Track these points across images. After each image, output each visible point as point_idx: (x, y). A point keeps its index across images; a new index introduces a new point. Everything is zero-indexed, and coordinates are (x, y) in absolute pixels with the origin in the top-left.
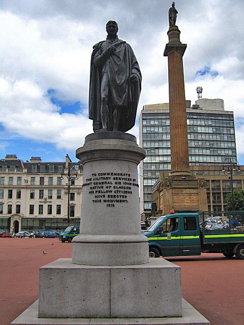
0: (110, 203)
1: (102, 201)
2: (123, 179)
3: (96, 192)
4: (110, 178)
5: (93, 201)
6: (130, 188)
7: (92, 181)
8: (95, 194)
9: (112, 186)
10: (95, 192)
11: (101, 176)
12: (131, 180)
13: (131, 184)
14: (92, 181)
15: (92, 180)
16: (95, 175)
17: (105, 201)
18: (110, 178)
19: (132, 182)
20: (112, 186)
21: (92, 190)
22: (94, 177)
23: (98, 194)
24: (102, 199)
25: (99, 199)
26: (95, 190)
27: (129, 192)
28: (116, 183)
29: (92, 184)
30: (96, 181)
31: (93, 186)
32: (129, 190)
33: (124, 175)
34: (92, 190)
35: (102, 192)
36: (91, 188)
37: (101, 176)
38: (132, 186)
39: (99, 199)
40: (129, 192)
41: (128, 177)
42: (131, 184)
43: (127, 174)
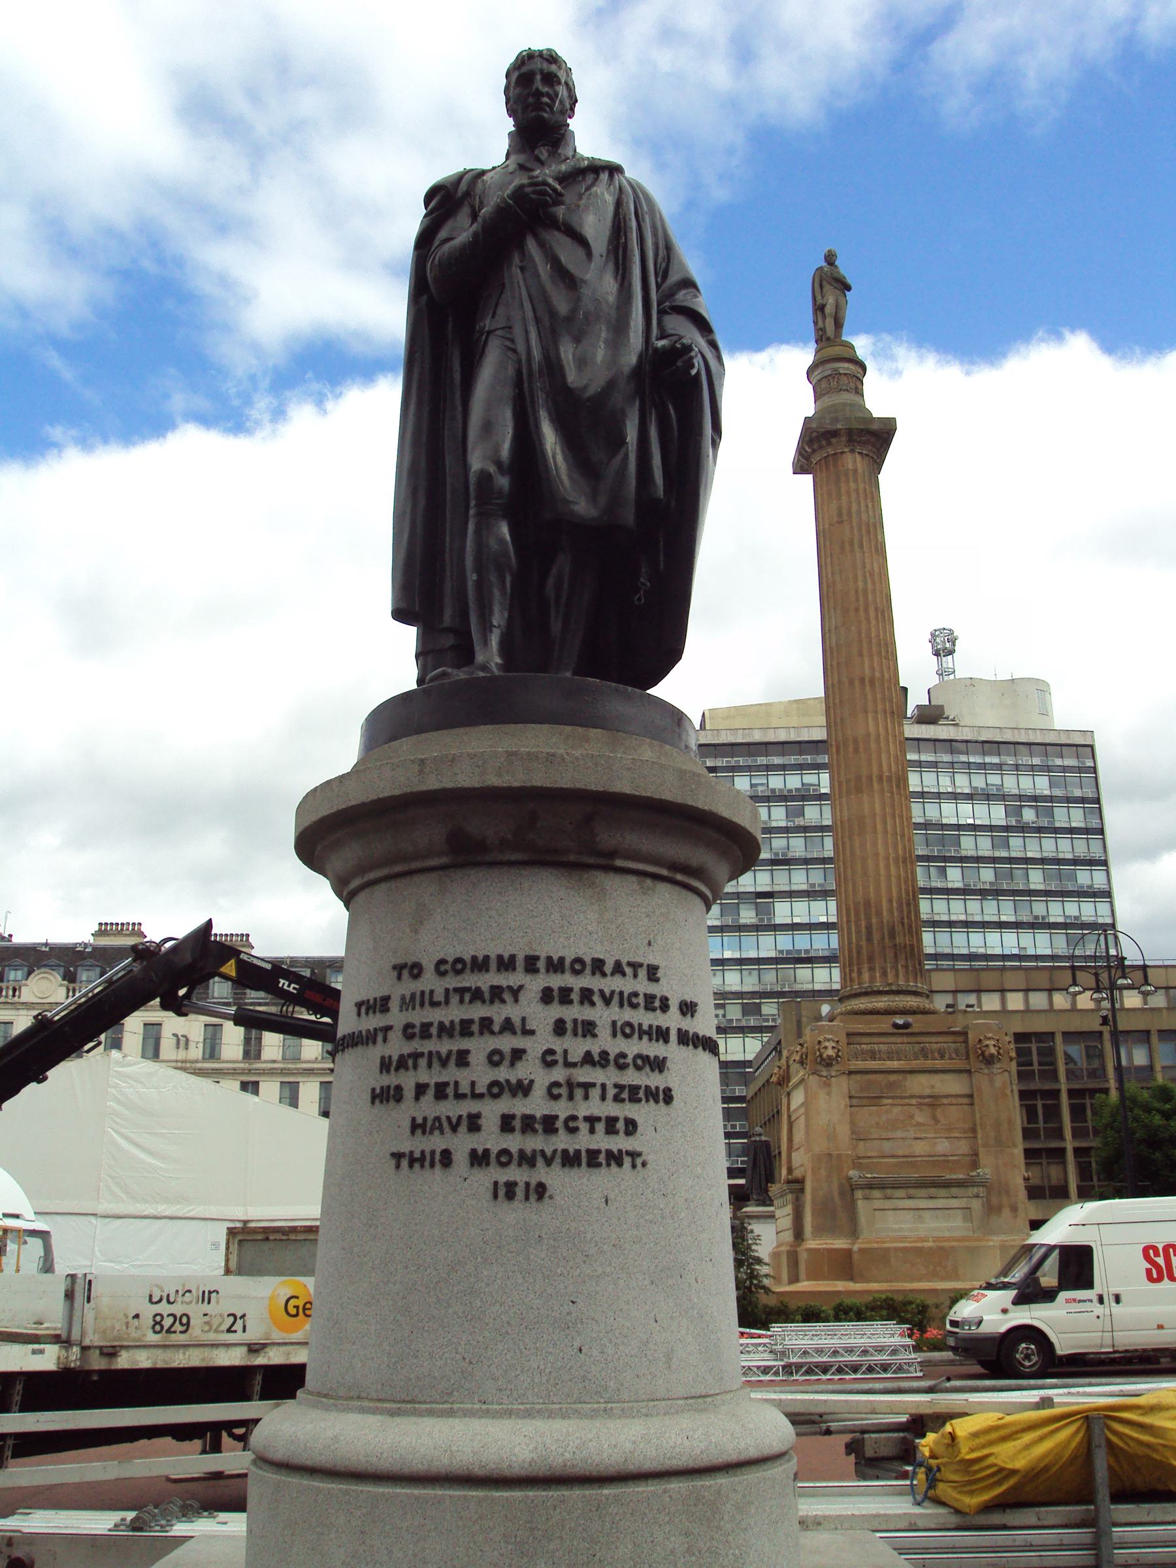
0: (515, 1174)
1: (461, 1157)
2: (607, 1001)
3: (421, 1089)
4: (516, 992)
5: (397, 1156)
6: (658, 1065)
7: (396, 1017)
8: (409, 1110)
9: (544, 1040)
10: (409, 1092)
11: (452, 982)
12: (665, 1006)
13: (662, 1035)
14: (396, 1017)
15: (394, 1005)
16: (416, 970)
17: (479, 1159)
18: (516, 992)
19: (672, 1020)
20: (535, 1047)
21: (391, 1080)
22: (409, 987)
23: (429, 1108)
24: (461, 1144)
25: (436, 1142)
26: (408, 1081)
27: (652, 1095)
28: (560, 1028)
29: (395, 1036)
30: (418, 1017)
31: (396, 1047)
32: (654, 1080)
33: (618, 969)
34: (391, 1080)
35: (459, 1096)
36: (385, 1065)
37: (452, 982)
38: (672, 1051)
39: (436, 1142)
40: (652, 1095)
41: (642, 986)
42: (662, 1035)
43: (635, 966)
